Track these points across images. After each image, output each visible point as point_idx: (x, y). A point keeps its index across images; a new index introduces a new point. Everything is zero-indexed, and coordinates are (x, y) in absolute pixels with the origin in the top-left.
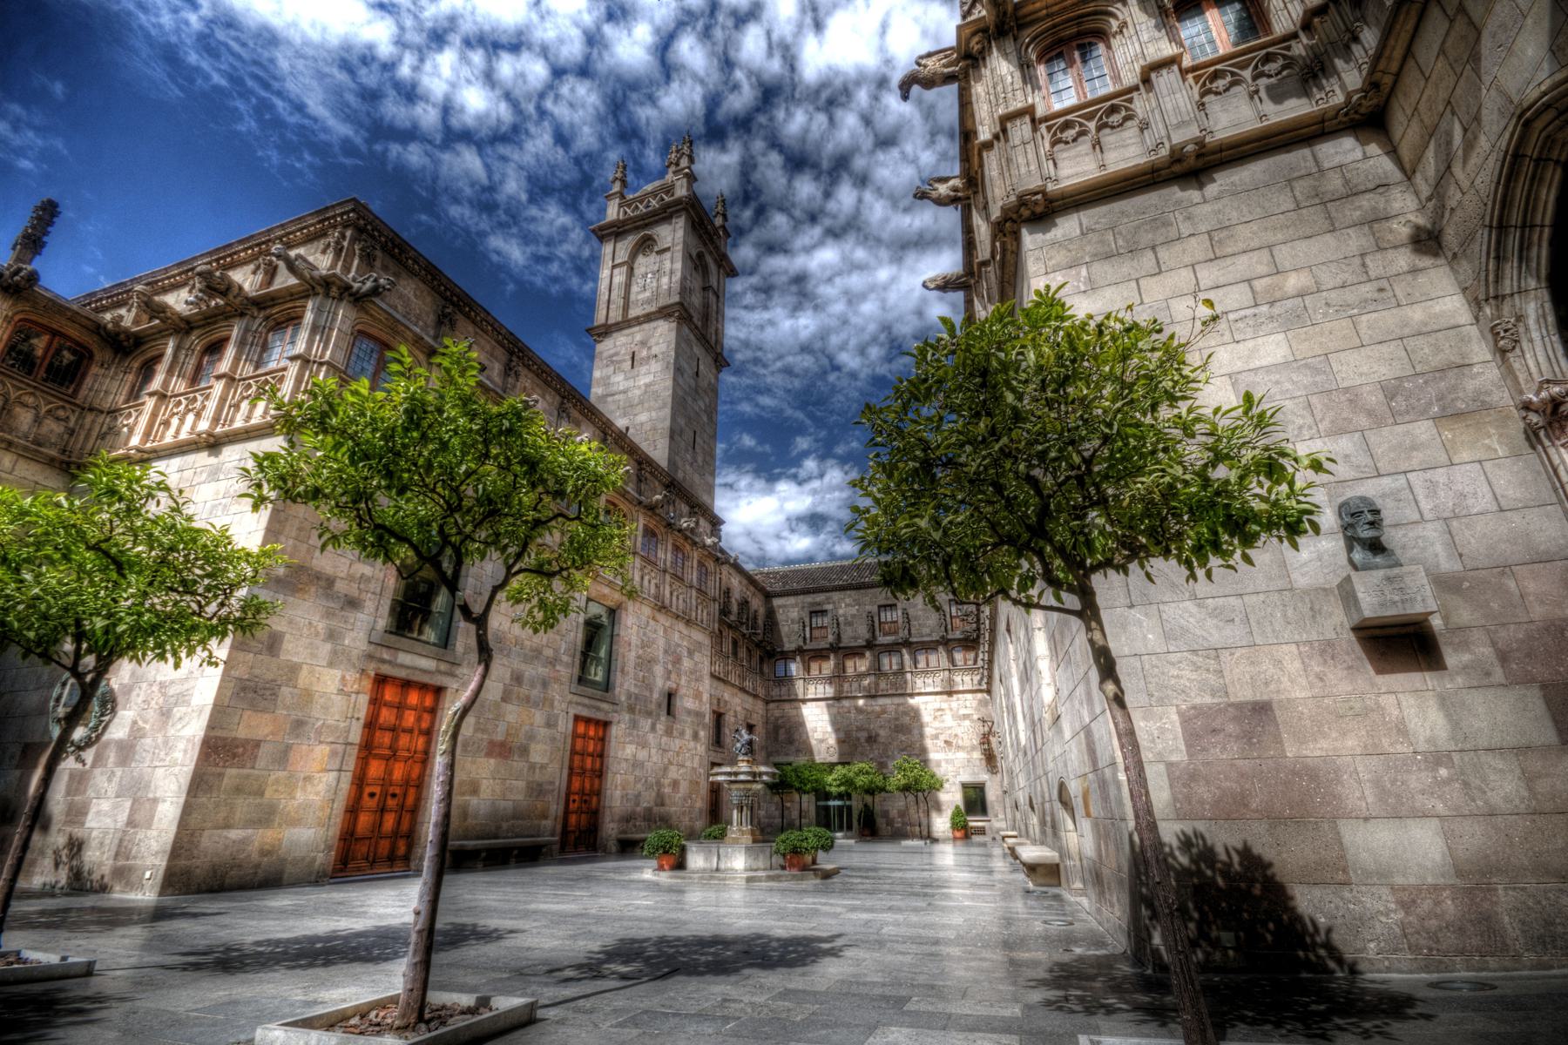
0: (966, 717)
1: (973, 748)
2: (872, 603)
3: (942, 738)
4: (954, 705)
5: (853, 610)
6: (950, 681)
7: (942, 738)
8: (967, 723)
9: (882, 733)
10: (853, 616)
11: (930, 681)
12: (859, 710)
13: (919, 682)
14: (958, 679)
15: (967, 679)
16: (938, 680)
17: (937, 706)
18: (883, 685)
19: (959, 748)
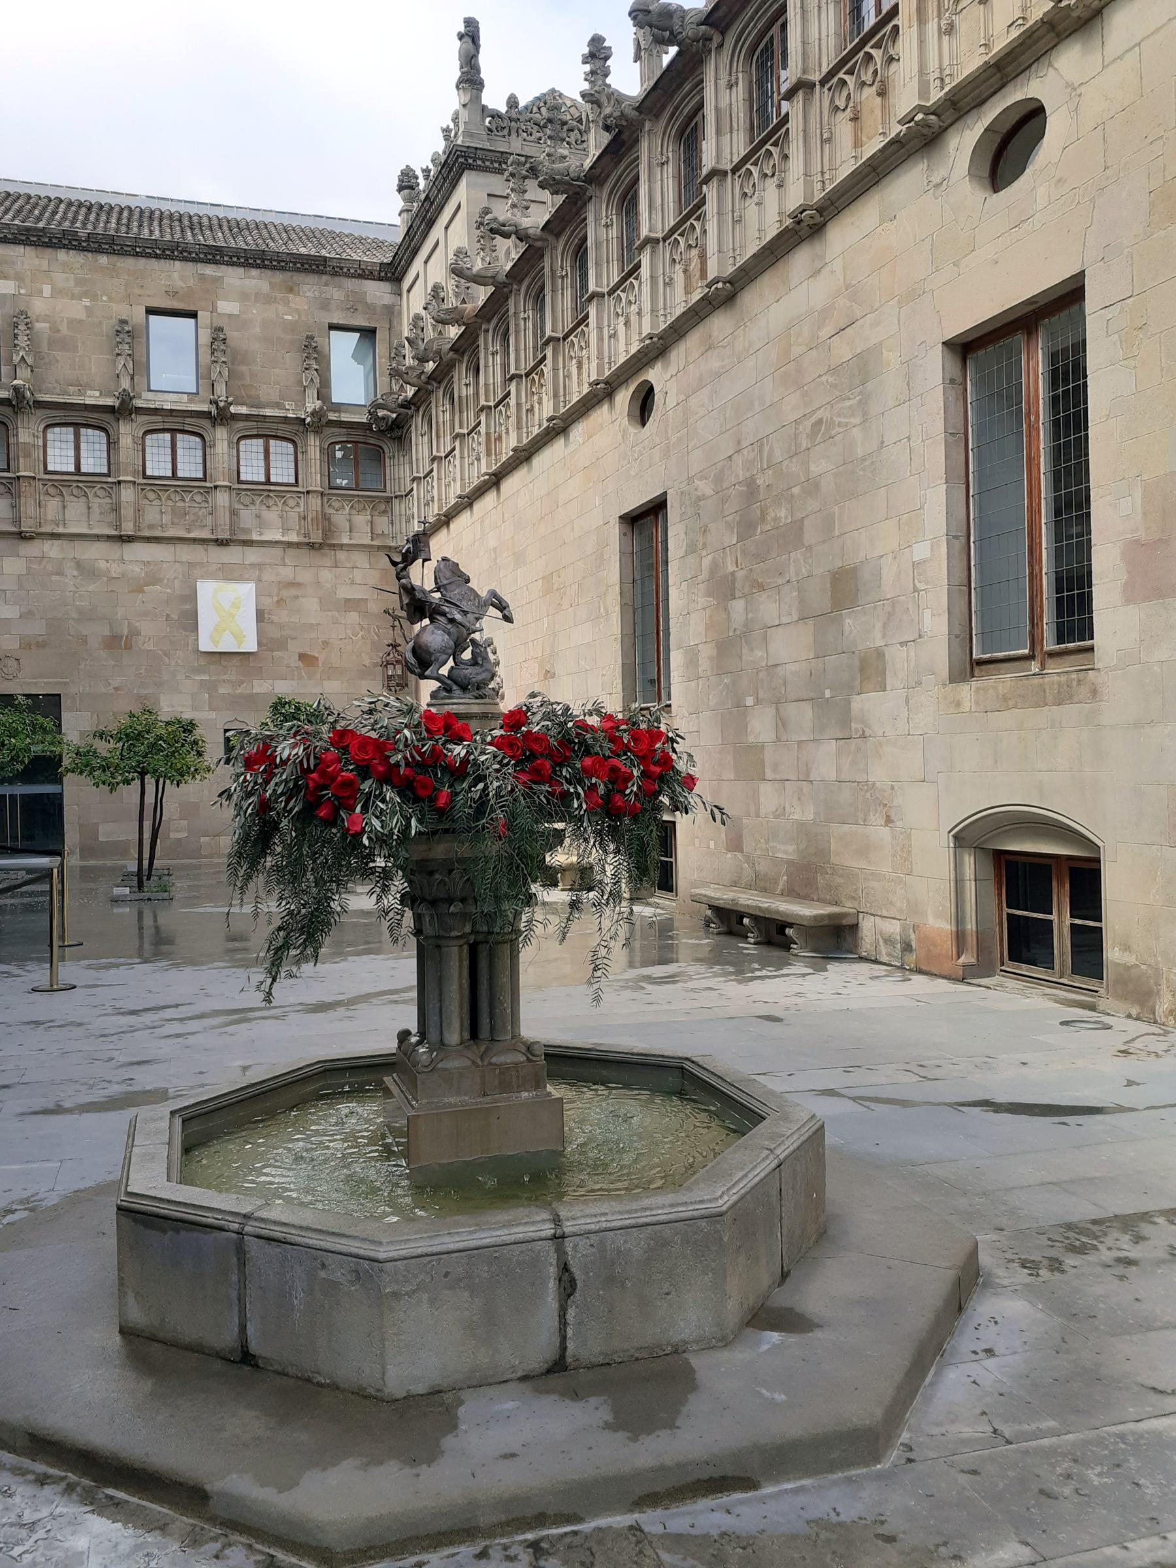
0: (350, 604)
1: (364, 673)
2: (129, 299)
3: (295, 647)
4: (326, 575)
5: (76, 309)
6: (326, 523)
7: (295, 647)
8: (353, 617)
9: (147, 628)
10: (74, 324)
11: (272, 516)
12: (87, 571)
13: (246, 517)
14: (340, 518)
15: (361, 520)
16: (293, 517)
17: (287, 573)
18: (152, 514)
19: (332, 672)
